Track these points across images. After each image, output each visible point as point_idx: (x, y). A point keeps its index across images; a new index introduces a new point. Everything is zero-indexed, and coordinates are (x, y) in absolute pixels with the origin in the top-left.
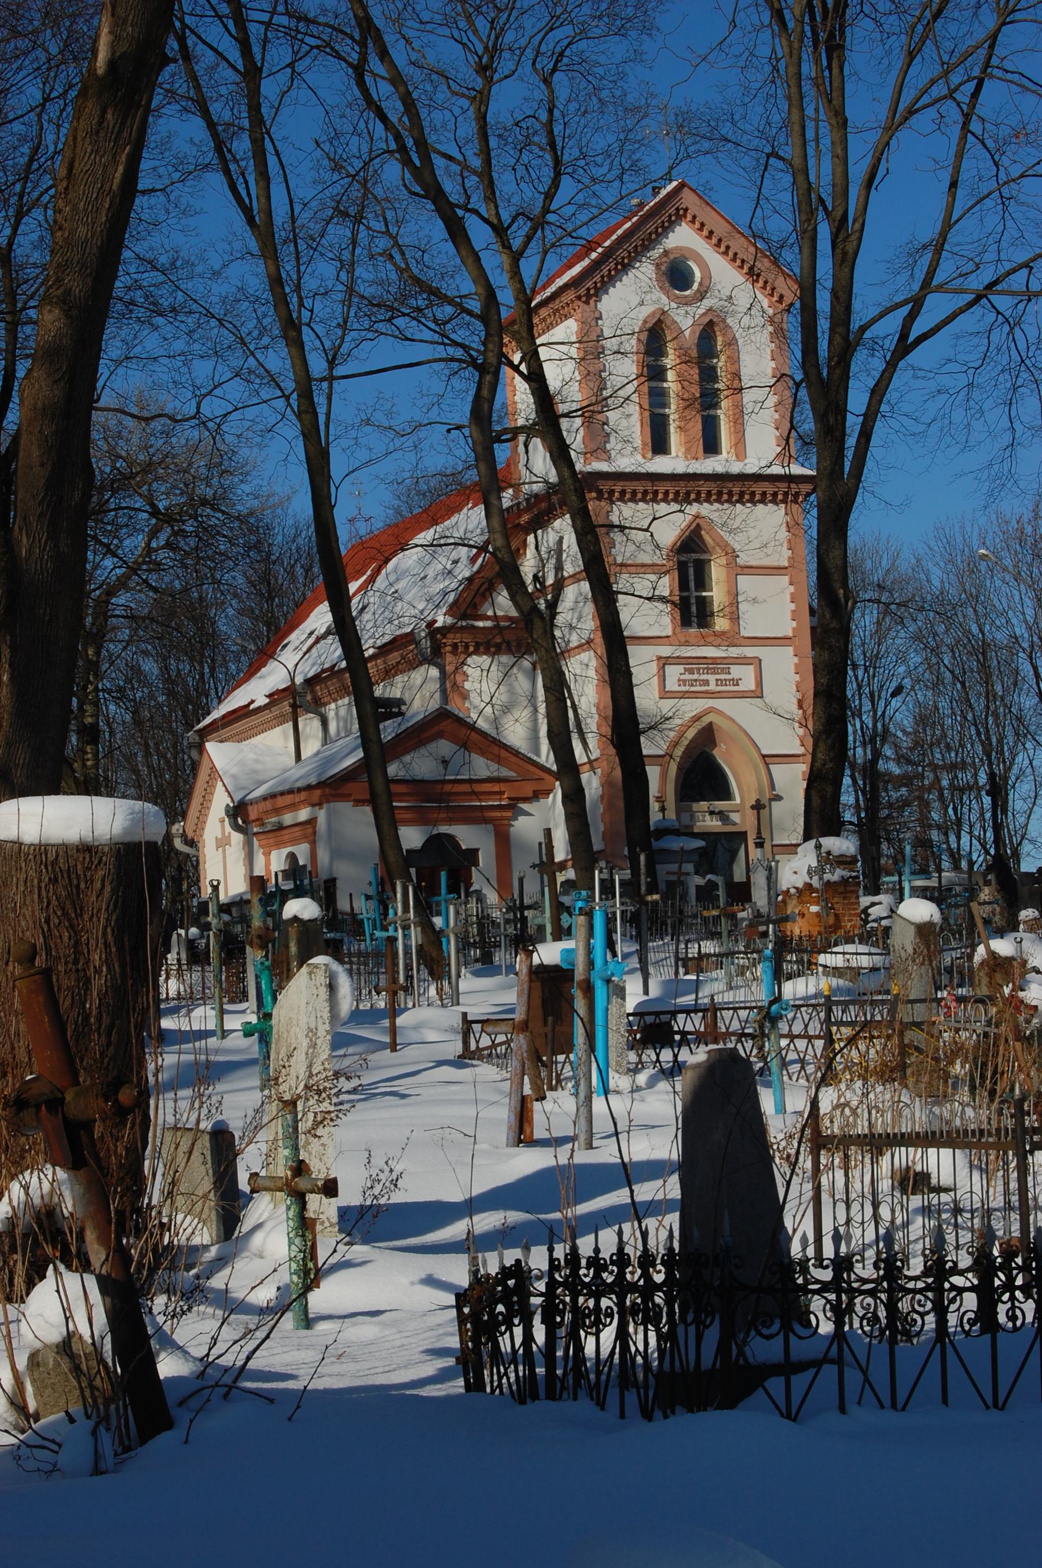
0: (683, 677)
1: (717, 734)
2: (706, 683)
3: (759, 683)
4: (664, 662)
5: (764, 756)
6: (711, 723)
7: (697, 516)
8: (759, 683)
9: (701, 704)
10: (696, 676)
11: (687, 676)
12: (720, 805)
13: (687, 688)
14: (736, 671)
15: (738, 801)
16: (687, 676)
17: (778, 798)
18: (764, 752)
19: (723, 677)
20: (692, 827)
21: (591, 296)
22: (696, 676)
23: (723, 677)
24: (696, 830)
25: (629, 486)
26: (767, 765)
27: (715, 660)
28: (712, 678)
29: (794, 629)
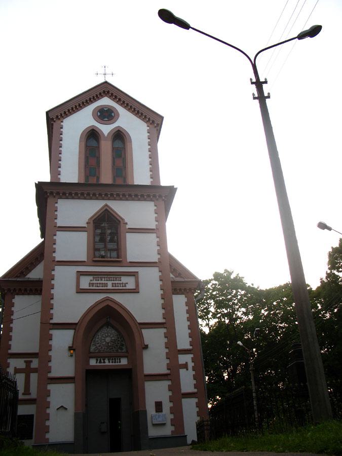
0: (92, 282)
2: (106, 285)
4: (80, 274)
7: (106, 205)
14: (124, 279)
16: (95, 282)
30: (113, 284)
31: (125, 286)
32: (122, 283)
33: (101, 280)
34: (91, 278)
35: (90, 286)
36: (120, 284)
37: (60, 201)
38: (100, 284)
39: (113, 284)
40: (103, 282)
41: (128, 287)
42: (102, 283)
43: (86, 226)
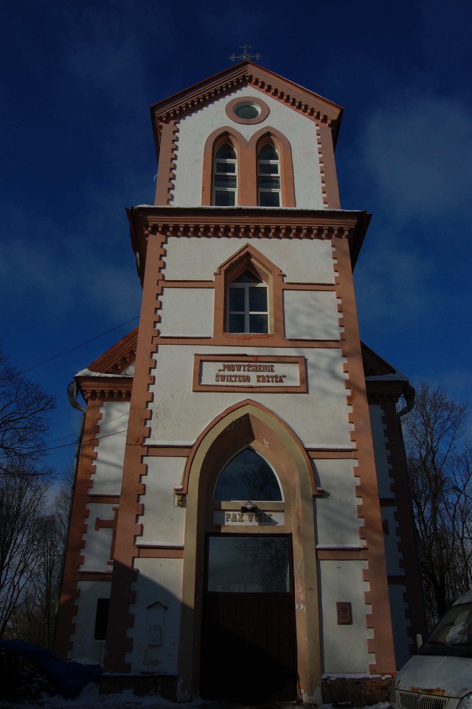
0: (221, 373)
1: (254, 426)
2: (247, 379)
3: (305, 379)
5: (307, 451)
6: (247, 416)
7: (247, 246)
8: (305, 379)
9: (240, 397)
10: (236, 373)
11: (227, 373)
12: (263, 504)
13: (226, 383)
14: (279, 369)
15: (283, 501)
16: (227, 373)
17: (323, 494)
18: (308, 446)
19: (265, 374)
20: (219, 527)
21: (170, 119)
22: (236, 373)
23: (265, 374)
24: (223, 530)
25: (182, 221)
26: (311, 459)
27: (256, 359)
28: (253, 375)
29: (342, 334)
30: (259, 377)
31: (281, 381)
32: (276, 376)
33: (239, 370)
34: (220, 365)
35: (218, 381)
36: (272, 377)
37: (172, 240)
38: (235, 377)
39: (259, 377)
40: (242, 373)
41: (287, 383)
42: (240, 376)
43: (214, 280)
